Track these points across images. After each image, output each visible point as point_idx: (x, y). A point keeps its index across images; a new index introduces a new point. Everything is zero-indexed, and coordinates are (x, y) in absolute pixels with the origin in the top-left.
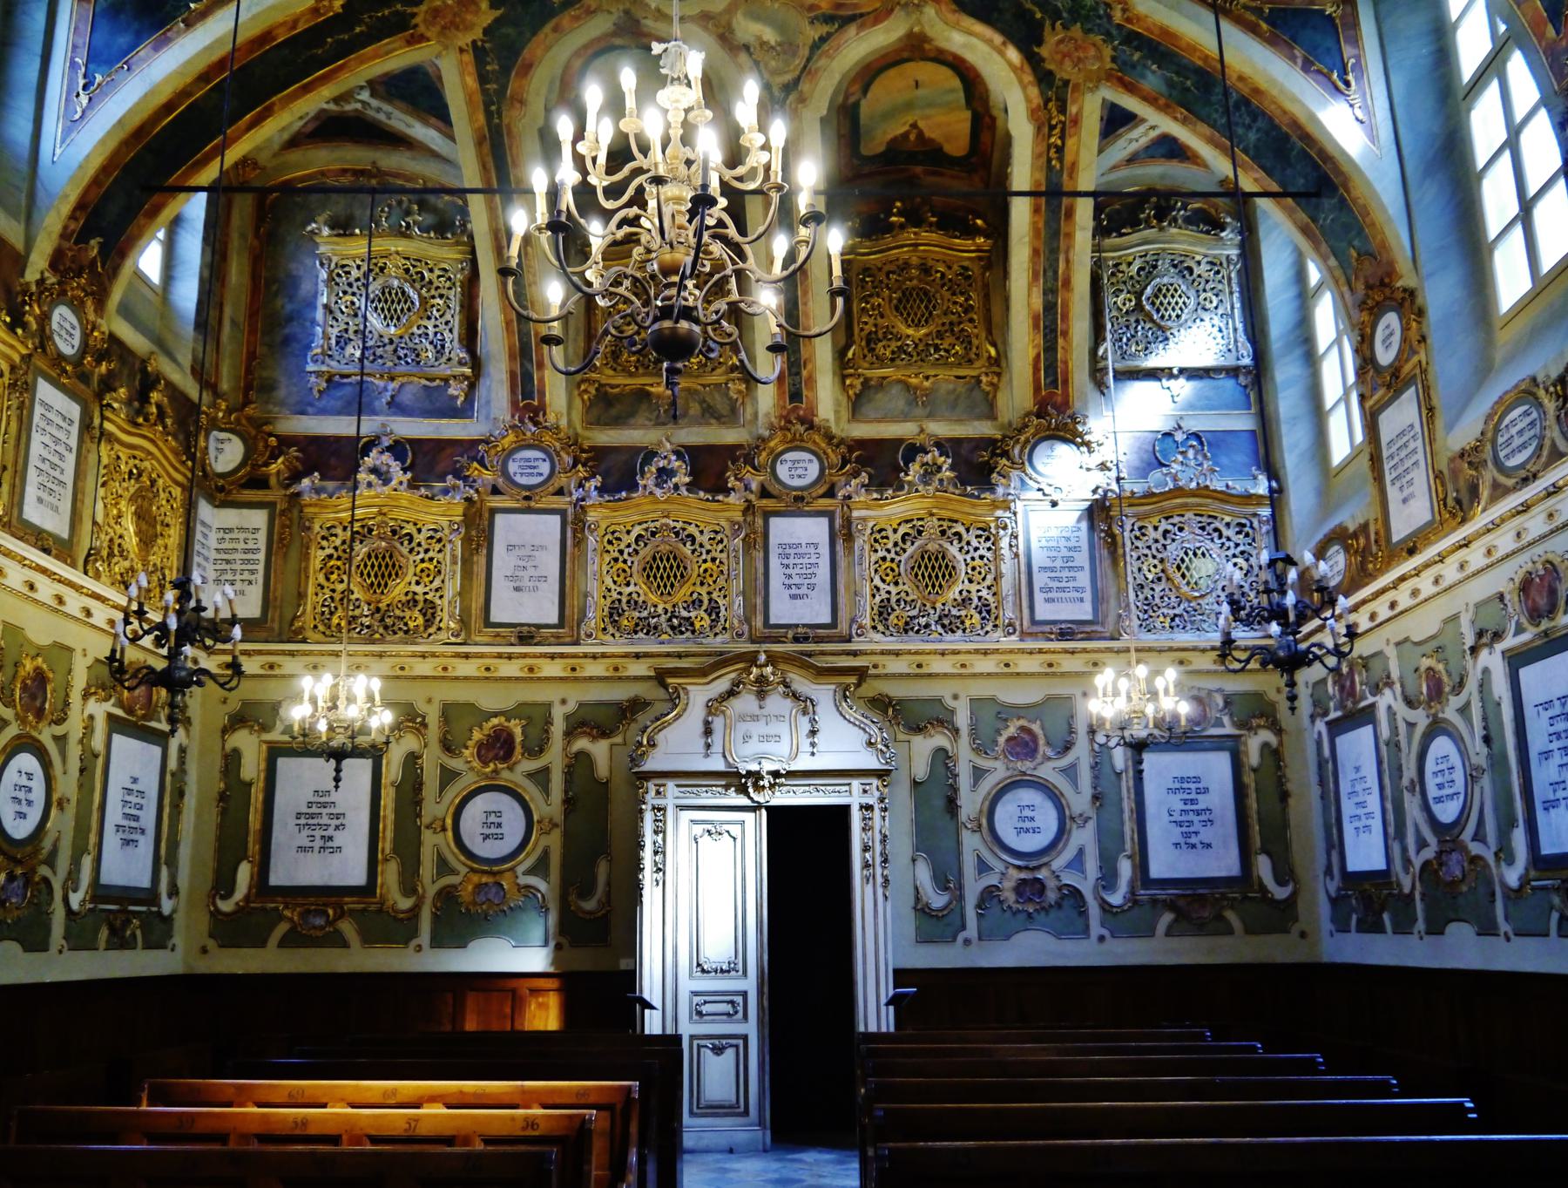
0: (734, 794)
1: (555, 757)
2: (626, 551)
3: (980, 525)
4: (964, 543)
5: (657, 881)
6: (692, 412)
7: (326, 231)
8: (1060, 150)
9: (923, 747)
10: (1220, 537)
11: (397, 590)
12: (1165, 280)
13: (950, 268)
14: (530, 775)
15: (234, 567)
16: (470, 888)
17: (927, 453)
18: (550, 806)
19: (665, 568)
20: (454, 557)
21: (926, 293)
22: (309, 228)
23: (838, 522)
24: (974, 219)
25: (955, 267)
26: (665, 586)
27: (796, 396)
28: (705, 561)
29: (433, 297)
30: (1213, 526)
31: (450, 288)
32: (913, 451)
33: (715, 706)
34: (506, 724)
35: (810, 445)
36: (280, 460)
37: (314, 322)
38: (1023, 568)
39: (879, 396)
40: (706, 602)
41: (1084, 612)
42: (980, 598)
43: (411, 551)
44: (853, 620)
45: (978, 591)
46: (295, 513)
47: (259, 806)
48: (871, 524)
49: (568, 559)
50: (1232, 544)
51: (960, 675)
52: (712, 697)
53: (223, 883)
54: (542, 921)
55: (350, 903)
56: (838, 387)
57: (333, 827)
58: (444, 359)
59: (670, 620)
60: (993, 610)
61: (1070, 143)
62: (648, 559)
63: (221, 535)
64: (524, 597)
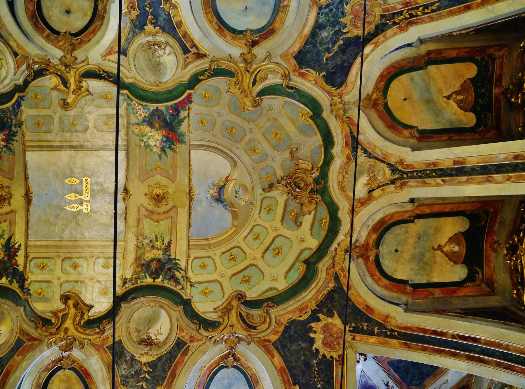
8: (426, 7)
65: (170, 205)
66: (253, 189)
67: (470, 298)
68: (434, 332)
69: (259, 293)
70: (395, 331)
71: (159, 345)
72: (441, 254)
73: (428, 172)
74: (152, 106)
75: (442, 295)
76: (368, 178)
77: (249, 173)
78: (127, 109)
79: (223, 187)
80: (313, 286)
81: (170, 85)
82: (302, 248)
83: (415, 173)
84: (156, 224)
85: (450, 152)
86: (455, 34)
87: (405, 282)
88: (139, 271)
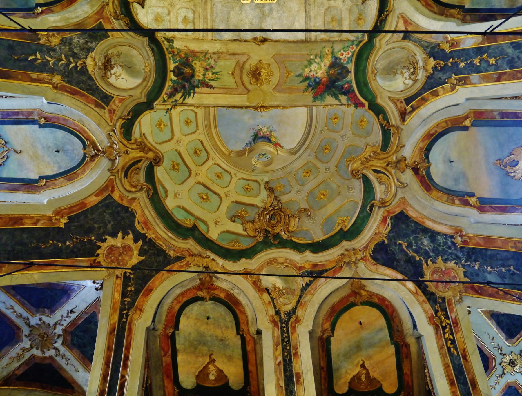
8: (453, 342)
61: (458, 337)
65: (250, 87)
66: (268, 172)
67: (162, 393)
68: (127, 358)
69: (162, 179)
70: (127, 318)
71: (104, 77)
72: (206, 363)
73: (288, 348)
74: (351, 67)
75: (164, 364)
76: (281, 288)
77: (284, 168)
78: (348, 40)
79: (270, 141)
80: (170, 235)
81: (373, 85)
82: (209, 223)
83: (286, 335)
84: (230, 73)
85: (309, 369)
86: (426, 371)
87: (176, 327)
88: (181, 55)
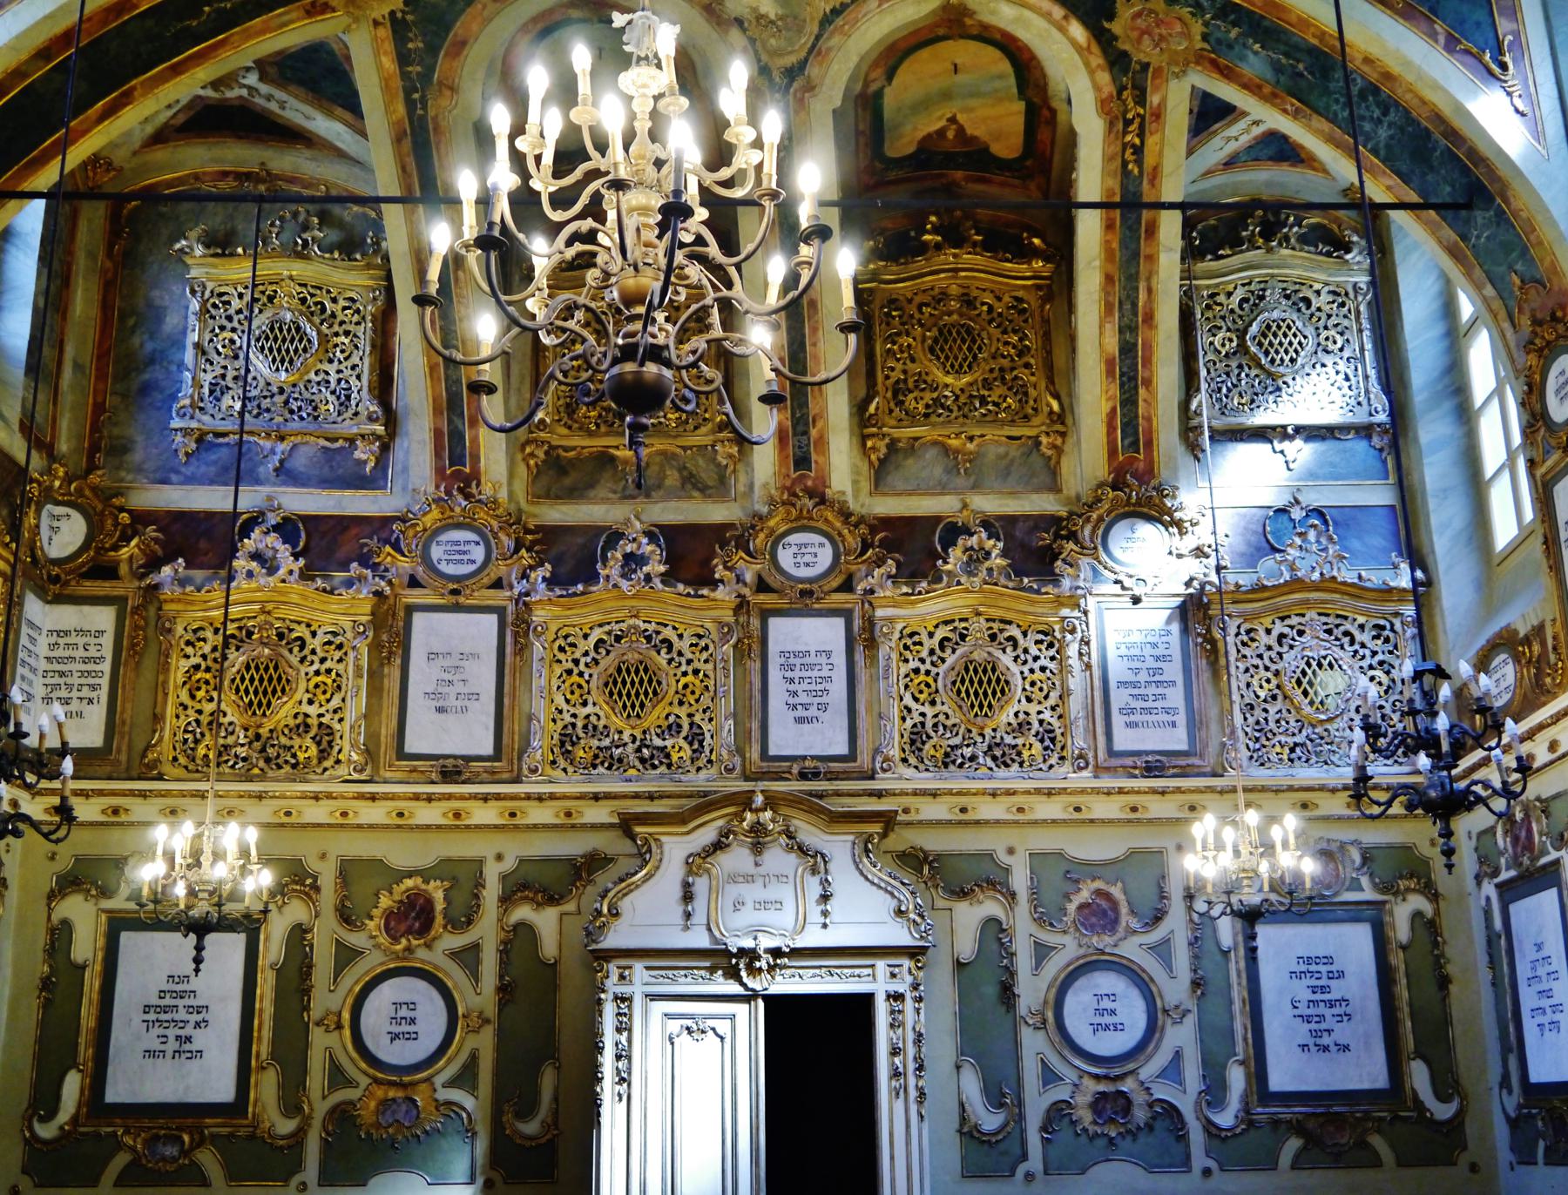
0: (721, 979)
1: (487, 930)
2: (583, 660)
3: (1040, 628)
4: (1020, 651)
5: (620, 1095)
6: (668, 482)
7: (199, 250)
8: (1138, 151)
9: (969, 916)
10: (1352, 643)
11: (283, 712)
12: (1275, 314)
13: (999, 299)
14: (455, 955)
15: (69, 680)
16: (373, 1104)
17: (971, 535)
18: (480, 996)
19: (633, 683)
20: (358, 668)
21: (969, 331)
22: (177, 246)
23: (857, 623)
24: (1029, 238)
25: (1006, 298)
26: (633, 706)
27: (802, 462)
28: (685, 674)
29: (337, 334)
30: (1342, 629)
31: (358, 323)
32: (954, 531)
33: (697, 863)
34: (423, 887)
35: (821, 525)
36: (133, 543)
37: (181, 366)
38: (1097, 683)
39: (910, 461)
40: (686, 727)
41: (1177, 740)
42: (1041, 722)
43: (302, 660)
44: (877, 751)
45: (1039, 713)
46: (152, 611)
47: (95, 996)
48: (899, 627)
49: (507, 671)
50: (1368, 652)
51: (1016, 822)
52: (694, 850)
53: (44, 1100)
54: (468, 1148)
55: (213, 1125)
56: (856, 452)
57: (192, 1024)
58: (351, 412)
59: (639, 750)
60: (1059, 738)
61: (1151, 142)
62: (611, 670)
63: (53, 639)
64: (449, 720)
76: (772, 16)
